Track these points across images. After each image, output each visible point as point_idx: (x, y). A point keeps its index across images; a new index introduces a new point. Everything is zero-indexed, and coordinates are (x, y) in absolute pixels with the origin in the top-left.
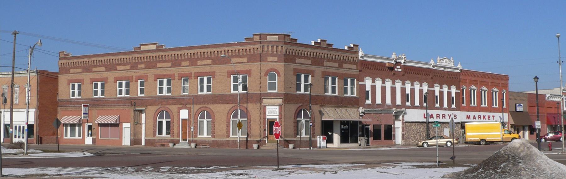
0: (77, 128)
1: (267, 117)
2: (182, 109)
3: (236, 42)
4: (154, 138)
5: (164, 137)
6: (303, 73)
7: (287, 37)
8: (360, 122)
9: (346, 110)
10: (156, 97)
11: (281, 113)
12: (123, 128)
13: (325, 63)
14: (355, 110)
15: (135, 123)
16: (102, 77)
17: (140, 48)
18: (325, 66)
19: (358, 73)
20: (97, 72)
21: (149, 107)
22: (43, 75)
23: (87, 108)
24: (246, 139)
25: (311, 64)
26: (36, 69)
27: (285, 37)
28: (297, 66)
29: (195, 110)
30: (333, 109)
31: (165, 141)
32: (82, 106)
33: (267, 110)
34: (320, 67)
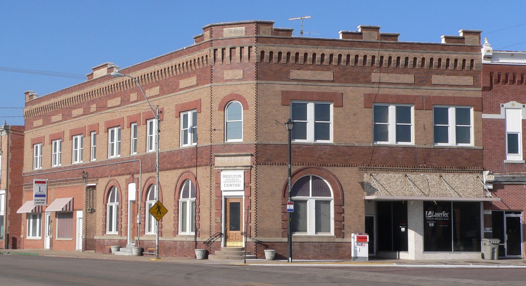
0: (38, 220)
1: (224, 194)
3: (185, 48)
5: (310, 237)
6: (311, 101)
7: (262, 28)
8: (488, 205)
9: (441, 176)
10: (106, 162)
11: (250, 185)
13: (375, 77)
14: (470, 178)
15: (88, 211)
17: (92, 74)
18: (374, 83)
19: (479, 94)
22: (18, 133)
23: (44, 187)
24: (193, 239)
25: (332, 79)
26: (6, 124)
27: (257, 28)
28: (291, 87)
29: (142, 186)
30: (399, 175)
32: (32, 184)
33: (223, 180)
34: (359, 85)
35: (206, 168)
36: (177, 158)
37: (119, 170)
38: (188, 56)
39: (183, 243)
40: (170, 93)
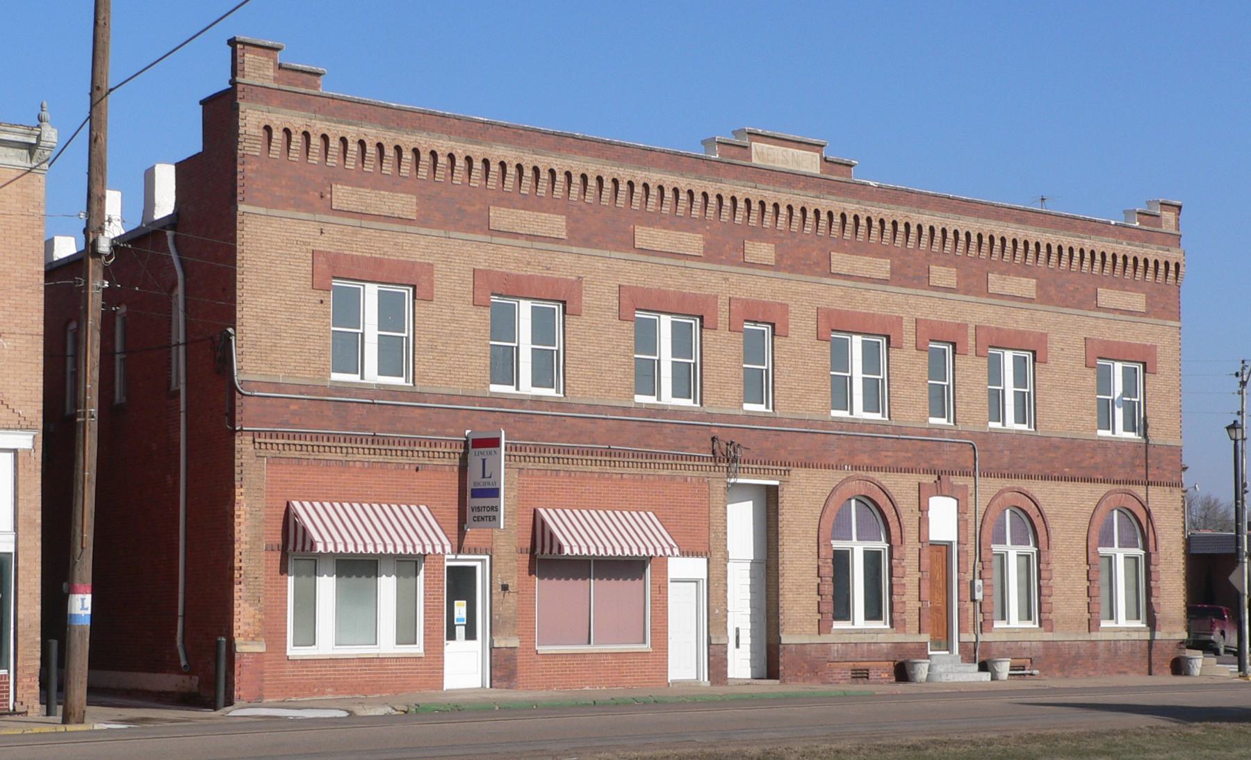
2: (940, 493)
3: (1113, 222)
4: (824, 638)
12: (670, 585)
16: (545, 274)
20: (516, 235)
21: (799, 474)
31: (869, 651)
35: (1171, 491)
36: (1092, 458)
37: (886, 456)
38: (1129, 245)
39: (1116, 645)
40: (1067, 307)
